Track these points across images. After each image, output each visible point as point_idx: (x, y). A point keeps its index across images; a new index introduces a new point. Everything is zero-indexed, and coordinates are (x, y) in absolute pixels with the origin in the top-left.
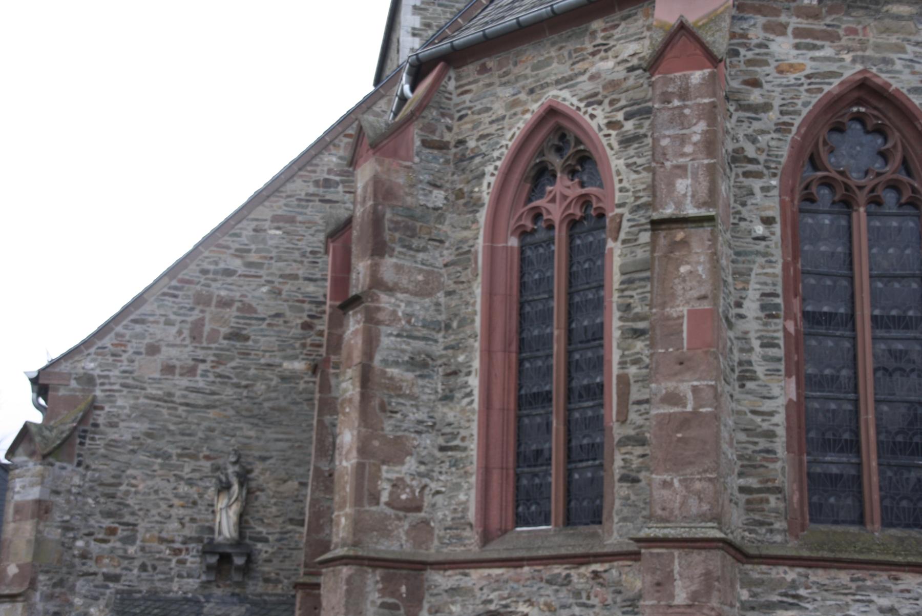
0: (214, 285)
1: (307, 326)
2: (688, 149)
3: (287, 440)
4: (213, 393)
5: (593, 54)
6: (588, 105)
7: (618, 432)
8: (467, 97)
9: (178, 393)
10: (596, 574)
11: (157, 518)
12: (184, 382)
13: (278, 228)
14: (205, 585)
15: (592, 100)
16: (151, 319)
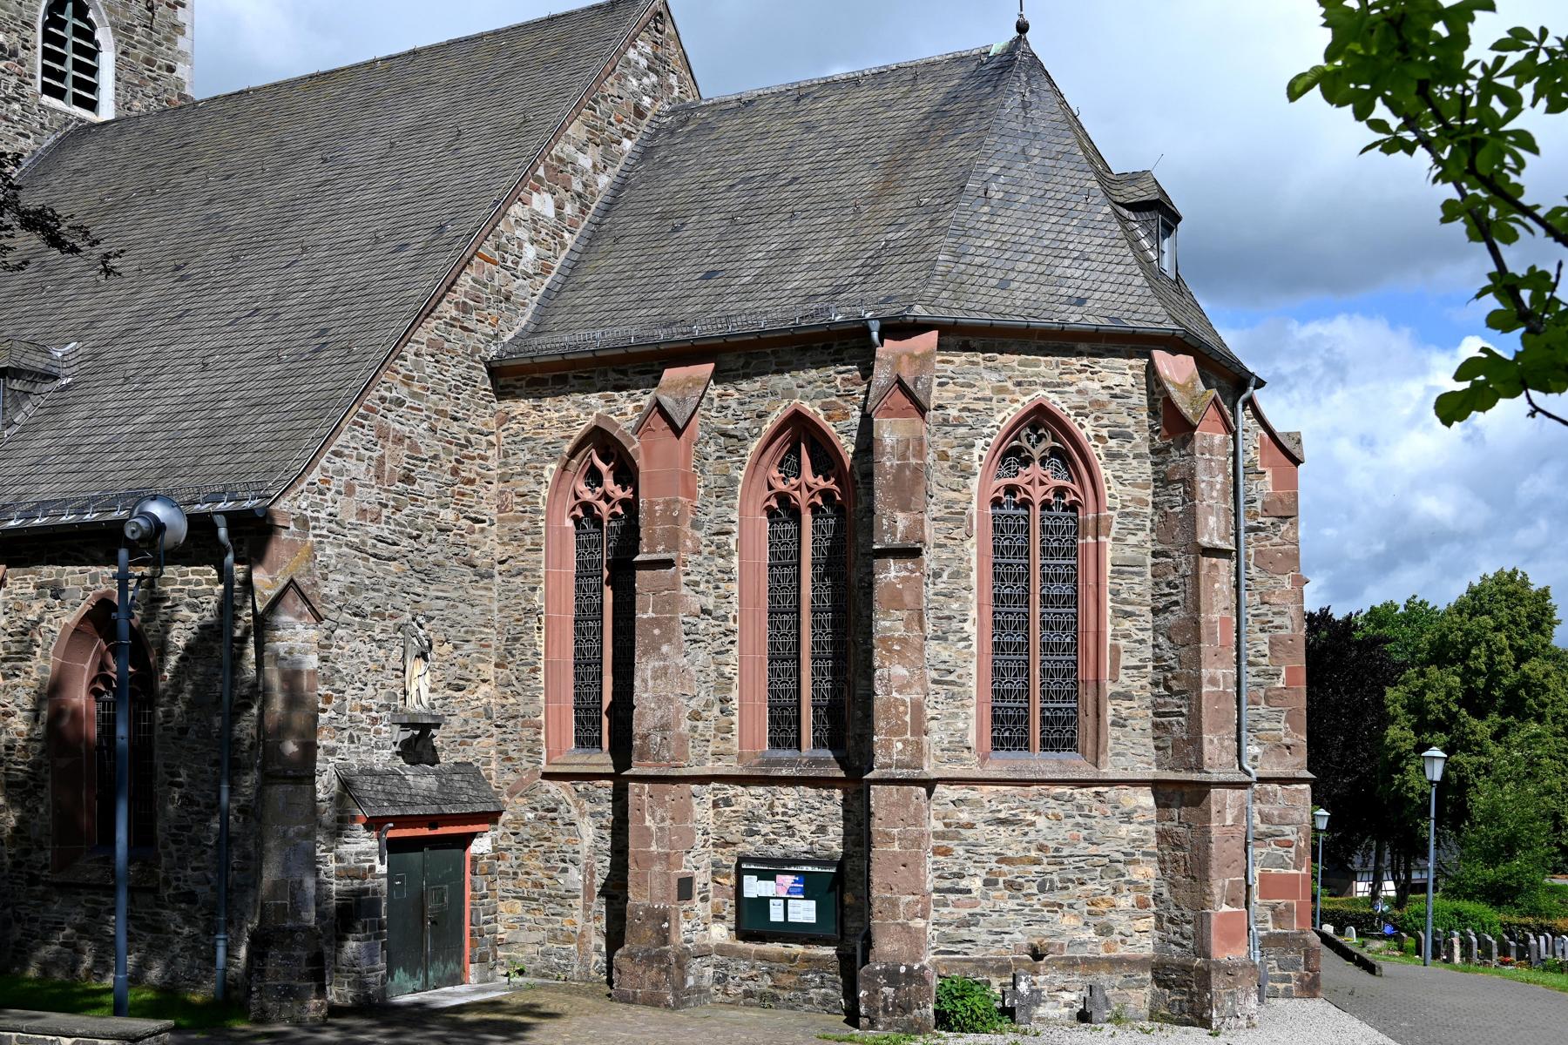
0: (390, 415)
1: (455, 472)
2: (1215, 494)
4: (395, 544)
5: (1080, 372)
6: (1077, 415)
7: (1110, 688)
8: (950, 367)
10: (1097, 793)
11: (359, 685)
12: (373, 529)
15: (1080, 412)
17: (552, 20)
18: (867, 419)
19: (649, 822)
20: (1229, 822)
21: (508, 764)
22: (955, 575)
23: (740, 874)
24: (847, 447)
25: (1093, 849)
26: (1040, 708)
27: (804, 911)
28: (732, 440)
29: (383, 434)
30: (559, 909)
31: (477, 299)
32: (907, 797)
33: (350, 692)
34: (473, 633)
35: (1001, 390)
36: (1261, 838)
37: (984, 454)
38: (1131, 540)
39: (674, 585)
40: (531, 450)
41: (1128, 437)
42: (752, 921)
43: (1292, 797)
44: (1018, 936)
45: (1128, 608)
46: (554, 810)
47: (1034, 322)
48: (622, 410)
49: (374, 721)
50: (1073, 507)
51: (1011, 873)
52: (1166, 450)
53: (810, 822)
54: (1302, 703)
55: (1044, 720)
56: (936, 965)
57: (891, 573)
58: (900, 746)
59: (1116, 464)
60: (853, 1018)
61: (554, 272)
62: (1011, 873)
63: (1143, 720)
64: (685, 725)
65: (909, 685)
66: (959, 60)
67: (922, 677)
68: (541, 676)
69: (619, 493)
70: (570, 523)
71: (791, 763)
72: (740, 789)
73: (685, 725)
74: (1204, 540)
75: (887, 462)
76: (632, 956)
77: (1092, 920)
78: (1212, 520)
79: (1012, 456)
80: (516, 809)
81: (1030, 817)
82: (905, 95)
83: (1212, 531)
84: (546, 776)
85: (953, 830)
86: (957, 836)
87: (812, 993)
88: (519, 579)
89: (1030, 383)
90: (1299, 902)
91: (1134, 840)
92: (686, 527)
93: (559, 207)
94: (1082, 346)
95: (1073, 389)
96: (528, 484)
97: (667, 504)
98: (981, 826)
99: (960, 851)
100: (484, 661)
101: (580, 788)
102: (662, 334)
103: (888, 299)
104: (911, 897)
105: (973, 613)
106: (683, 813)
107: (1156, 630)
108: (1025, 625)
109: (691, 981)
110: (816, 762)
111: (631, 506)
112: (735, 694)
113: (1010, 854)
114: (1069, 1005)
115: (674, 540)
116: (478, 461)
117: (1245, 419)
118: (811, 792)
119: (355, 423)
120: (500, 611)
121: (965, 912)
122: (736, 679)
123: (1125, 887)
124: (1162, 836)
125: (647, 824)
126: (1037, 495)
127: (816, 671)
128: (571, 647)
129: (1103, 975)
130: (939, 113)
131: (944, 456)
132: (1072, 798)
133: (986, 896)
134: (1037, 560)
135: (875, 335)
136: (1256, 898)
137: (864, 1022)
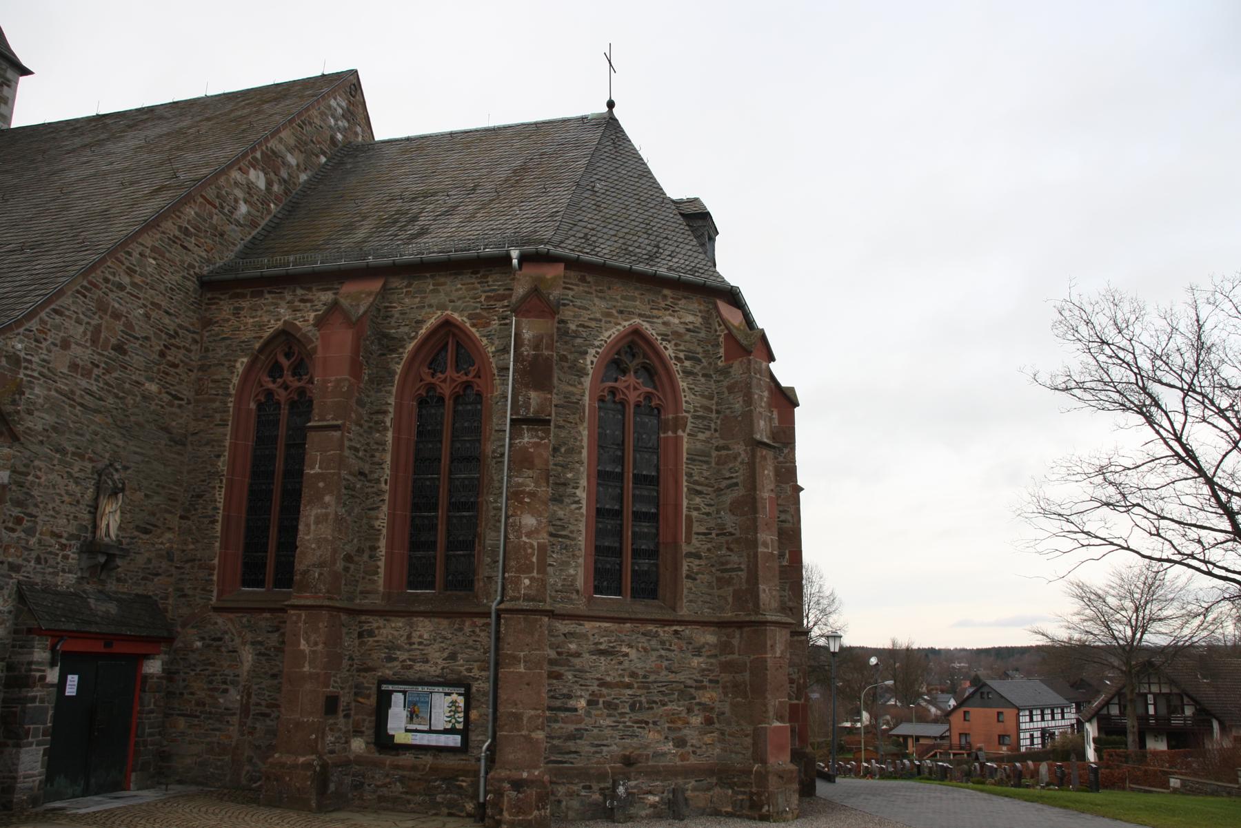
0: (111, 294)
1: (162, 354)
3: (142, 454)
4: (101, 399)
7: (685, 549)
8: (571, 293)
9: (78, 392)
10: (676, 632)
11: (51, 512)
12: (84, 383)
13: (154, 259)
14: (80, 580)
15: (665, 337)
16: (67, 313)
20: (778, 655)
21: (183, 600)
25: (671, 677)
29: (102, 307)
30: (218, 725)
33: (42, 517)
34: (164, 487)
35: (609, 315)
37: (595, 360)
38: (701, 436)
40: (227, 347)
44: (614, 748)
45: (699, 488)
46: (220, 639)
49: (63, 547)
51: (609, 695)
58: (527, 582)
59: (690, 379)
61: (259, 228)
62: (609, 695)
68: (218, 527)
70: (253, 406)
72: (381, 622)
74: (758, 437)
77: (672, 736)
78: (762, 423)
81: (625, 649)
84: (216, 609)
86: (567, 663)
88: (207, 449)
89: (629, 313)
91: (704, 670)
93: (269, 184)
95: (660, 321)
100: (171, 512)
101: (244, 620)
104: (532, 712)
105: (584, 482)
113: (608, 679)
116: (183, 351)
119: (78, 292)
120: (189, 472)
121: (571, 727)
122: (384, 531)
123: (696, 708)
125: (302, 647)
126: (632, 397)
129: (680, 781)
132: (656, 635)
133: (588, 714)
135: (515, 262)
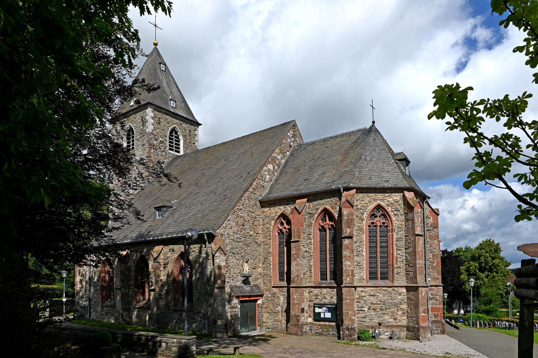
1: (253, 224)
7: (395, 266)
12: (236, 236)
17: (272, 128)
18: (340, 209)
19: (295, 296)
22: (360, 242)
23: (314, 307)
24: (336, 215)
25: (392, 301)
26: (380, 271)
27: (328, 315)
28: (311, 215)
29: (238, 216)
31: (257, 187)
32: (350, 290)
33: (232, 270)
36: (431, 299)
39: (299, 246)
41: (399, 211)
42: (317, 317)
43: (438, 289)
47: (377, 186)
48: (288, 209)
49: (237, 276)
50: (387, 226)
52: (408, 213)
53: (329, 296)
54: (440, 268)
55: (381, 273)
56: (357, 327)
57: (346, 242)
60: (339, 338)
63: (403, 273)
64: (302, 276)
65: (350, 266)
66: (360, 130)
67: (353, 264)
68: (272, 266)
69: (287, 227)
70: (277, 234)
71: (325, 283)
73: (302, 276)
75: (345, 218)
76: (291, 325)
79: (373, 216)
80: (267, 294)
81: (378, 294)
82: (348, 139)
83: (418, 231)
84: (273, 287)
85: (361, 297)
86: (362, 299)
87: (330, 333)
90: (440, 313)
92: (302, 234)
93: (274, 167)
94: (388, 191)
96: (268, 226)
97: (298, 229)
98: (367, 296)
99: (362, 302)
102: (296, 193)
103: (345, 183)
106: (302, 294)
107: (406, 253)
108: (376, 252)
109: (304, 330)
110: (330, 283)
111: (290, 230)
112: (313, 269)
114: (387, 335)
115: (299, 236)
117: (426, 206)
118: (329, 289)
121: (364, 315)
124: (408, 298)
127: (330, 264)
128: (278, 260)
129: (395, 329)
130: (355, 142)
131: (357, 216)
132: (387, 290)
133: (368, 312)
134: (379, 238)
136: (430, 312)
137: (342, 339)
